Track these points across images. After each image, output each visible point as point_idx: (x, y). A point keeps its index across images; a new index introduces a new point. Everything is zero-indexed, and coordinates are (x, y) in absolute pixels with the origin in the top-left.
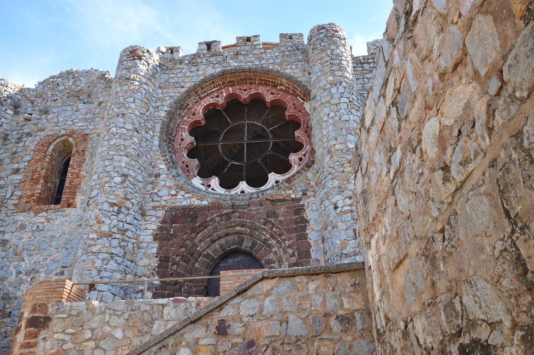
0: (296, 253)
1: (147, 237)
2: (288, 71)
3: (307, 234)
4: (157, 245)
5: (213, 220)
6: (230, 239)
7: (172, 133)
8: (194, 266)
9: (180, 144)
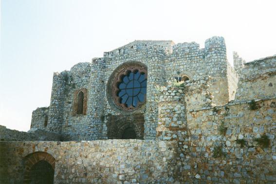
2: (144, 62)
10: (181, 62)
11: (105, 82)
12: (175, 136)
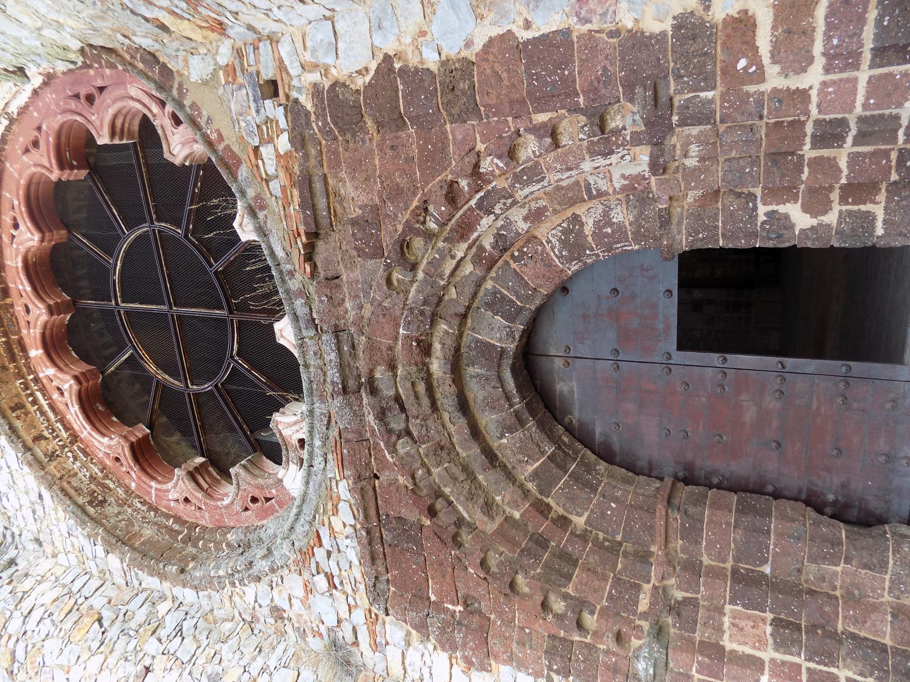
0: (541, 118)
3: (444, 64)
5: (405, 466)
6: (481, 394)
7: (170, 530)
8: (583, 537)
9: (200, 508)
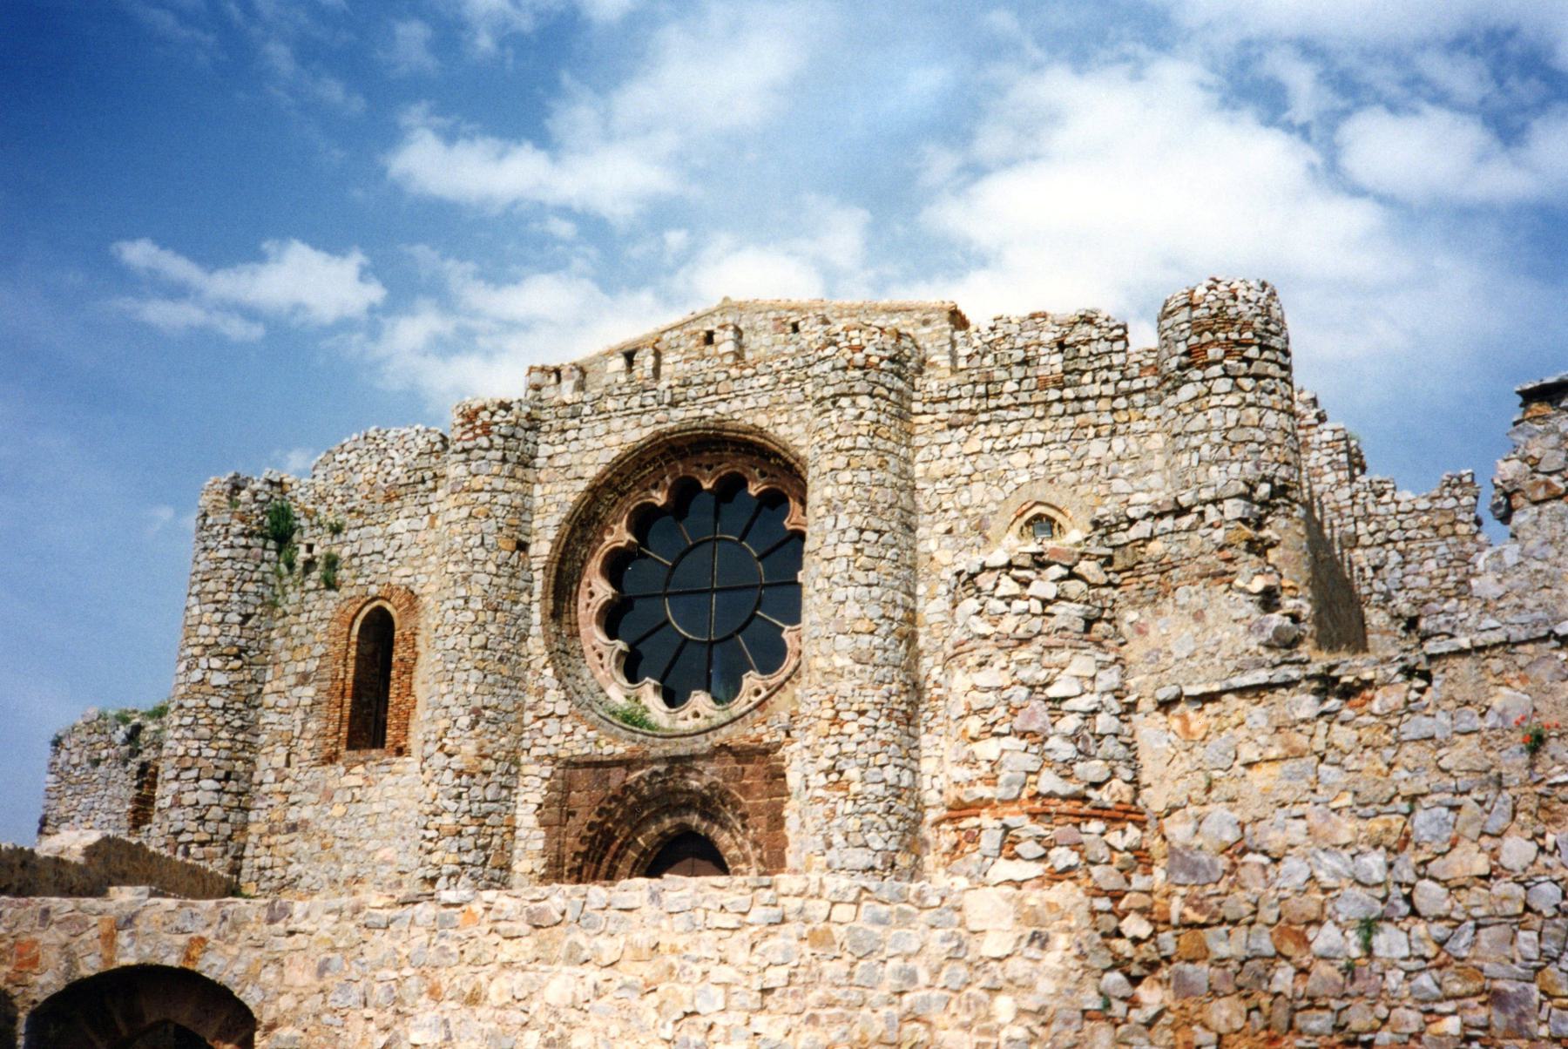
1: (526, 818)
2: (782, 431)
4: (543, 834)
10: (1013, 428)
11: (532, 550)
12: (1063, 857)
